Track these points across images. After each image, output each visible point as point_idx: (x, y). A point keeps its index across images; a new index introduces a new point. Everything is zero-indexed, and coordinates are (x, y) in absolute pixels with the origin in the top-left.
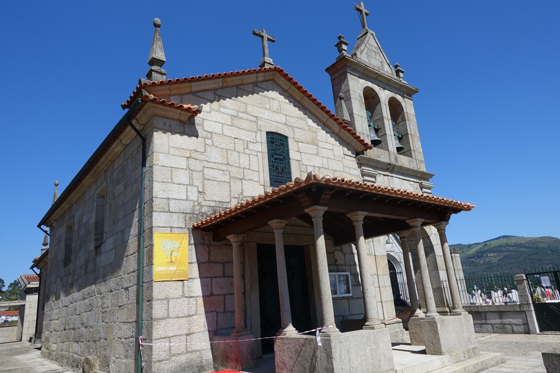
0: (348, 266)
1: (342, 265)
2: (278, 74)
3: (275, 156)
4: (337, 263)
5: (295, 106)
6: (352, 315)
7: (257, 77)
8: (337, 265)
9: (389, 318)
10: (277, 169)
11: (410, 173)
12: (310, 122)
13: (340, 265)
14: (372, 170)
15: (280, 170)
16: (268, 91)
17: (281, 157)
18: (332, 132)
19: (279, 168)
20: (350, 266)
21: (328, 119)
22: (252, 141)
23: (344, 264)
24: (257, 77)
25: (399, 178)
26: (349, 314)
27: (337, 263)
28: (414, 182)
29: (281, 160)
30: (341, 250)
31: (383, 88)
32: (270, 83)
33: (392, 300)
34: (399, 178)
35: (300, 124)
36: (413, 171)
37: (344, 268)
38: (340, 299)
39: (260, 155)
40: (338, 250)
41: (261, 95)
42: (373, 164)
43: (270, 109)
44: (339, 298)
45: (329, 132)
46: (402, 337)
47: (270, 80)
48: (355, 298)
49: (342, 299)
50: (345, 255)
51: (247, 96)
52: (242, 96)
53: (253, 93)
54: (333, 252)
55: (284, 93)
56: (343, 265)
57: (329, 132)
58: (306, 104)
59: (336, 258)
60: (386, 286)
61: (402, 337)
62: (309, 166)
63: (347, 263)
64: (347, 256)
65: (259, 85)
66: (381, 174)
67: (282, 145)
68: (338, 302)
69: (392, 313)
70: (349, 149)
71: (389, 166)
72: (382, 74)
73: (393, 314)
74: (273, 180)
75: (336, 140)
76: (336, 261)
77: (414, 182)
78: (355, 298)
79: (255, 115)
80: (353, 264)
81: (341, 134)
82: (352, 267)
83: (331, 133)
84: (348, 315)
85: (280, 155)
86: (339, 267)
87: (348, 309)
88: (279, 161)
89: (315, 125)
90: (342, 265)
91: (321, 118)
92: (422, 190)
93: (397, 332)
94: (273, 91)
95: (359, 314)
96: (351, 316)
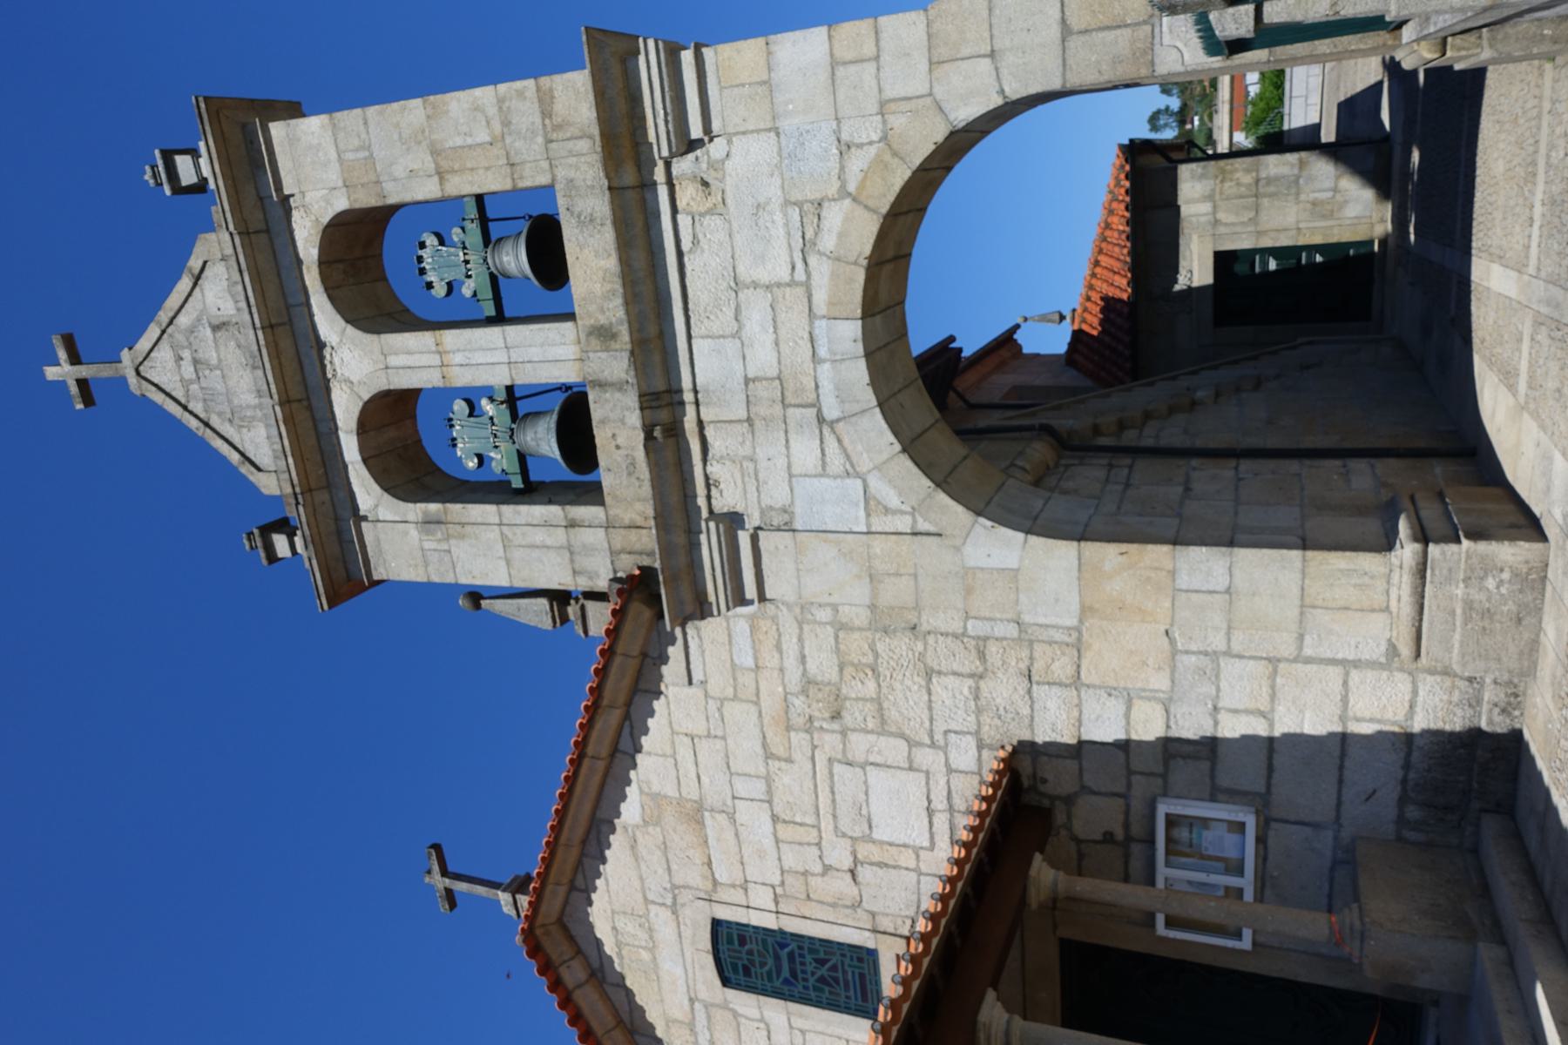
0: (1129, 785)
1: (1127, 813)
2: (540, 920)
3: (786, 973)
4: (1119, 834)
5: (604, 861)
6: (1338, 817)
7: (579, 986)
8: (1129, 839)
9: (1387, 609)
10: (822, 980)
11: (640, 258)
12: (631, 810)
13: (1126, 826)
14: (703, 538)
15: (823, 971)
16: (598, 943)
17: (784, 953)
18: (627, 723)
19: (819, 973)
20: (1130, 772)
21: (593, 757)
22: (765, 1033)
23: (1121, 801)
24: (579, 986)
25: (689, 337)
26: (1329, 834)
27: (1119, 834)
28: (674, 211)
29: (791, 956)
30: (1069, 800)
31: (322, 358)
32: (576, 930)
33: (1298, 564)
34: (689, 337)
35: (649, 841)
36: (621, 224)
37: (1137, 806)
38: (1265, 859)
39: (798, 1023)
40: (1069, 817)
41: (621, 965)
42: (680, 539)
43: (652, 950)
44: (1260, 861)
45: (632, 734)
46: (1506, 576)
47: (565, 929)
48: (1269, 786)
49: (1266, 848)
50: (1085, 789)
51: (642, 1011)
52: (652, 1027)
53: (629, 994)
54: (1078, 841)
55: (581, 884)
56: (1128, 806)
57: (632, 734)
58: (580, 832)
59: (1099, 837)
60: (1228, 591)
61: (1506, 576)
62: (780, 859)
63: (1120, 787)
64: (1089, 780)
65: (596, 965)
66: (707, 478)
67: (742, 941)
68: (1276, 874)
69: (1366, 580)
70: (664, 659)
71: (657, 433)
72: (276, 397)
73: (1372, 577)
74: (860, 1003)
75: (652, 713)
76: (1108, 838)
77: (674, 211)
78: (1269, 786)
79: (686, 1002)
80: (1121, 755)
81: (622, 699)
82: (1136, 764)
83: (632, 727)
84: (1336, 838)
85: (777, 958)
86: (1137, 830)
87: (1308, 831)
88: (798, 960)
89: (632, 791)
90: (1127, 813)
91: (597, 779)
92: (698, 144)
93: (1469, 605)
94: (591, 927)
95: (1341, 781)
96: (1341, 826)
